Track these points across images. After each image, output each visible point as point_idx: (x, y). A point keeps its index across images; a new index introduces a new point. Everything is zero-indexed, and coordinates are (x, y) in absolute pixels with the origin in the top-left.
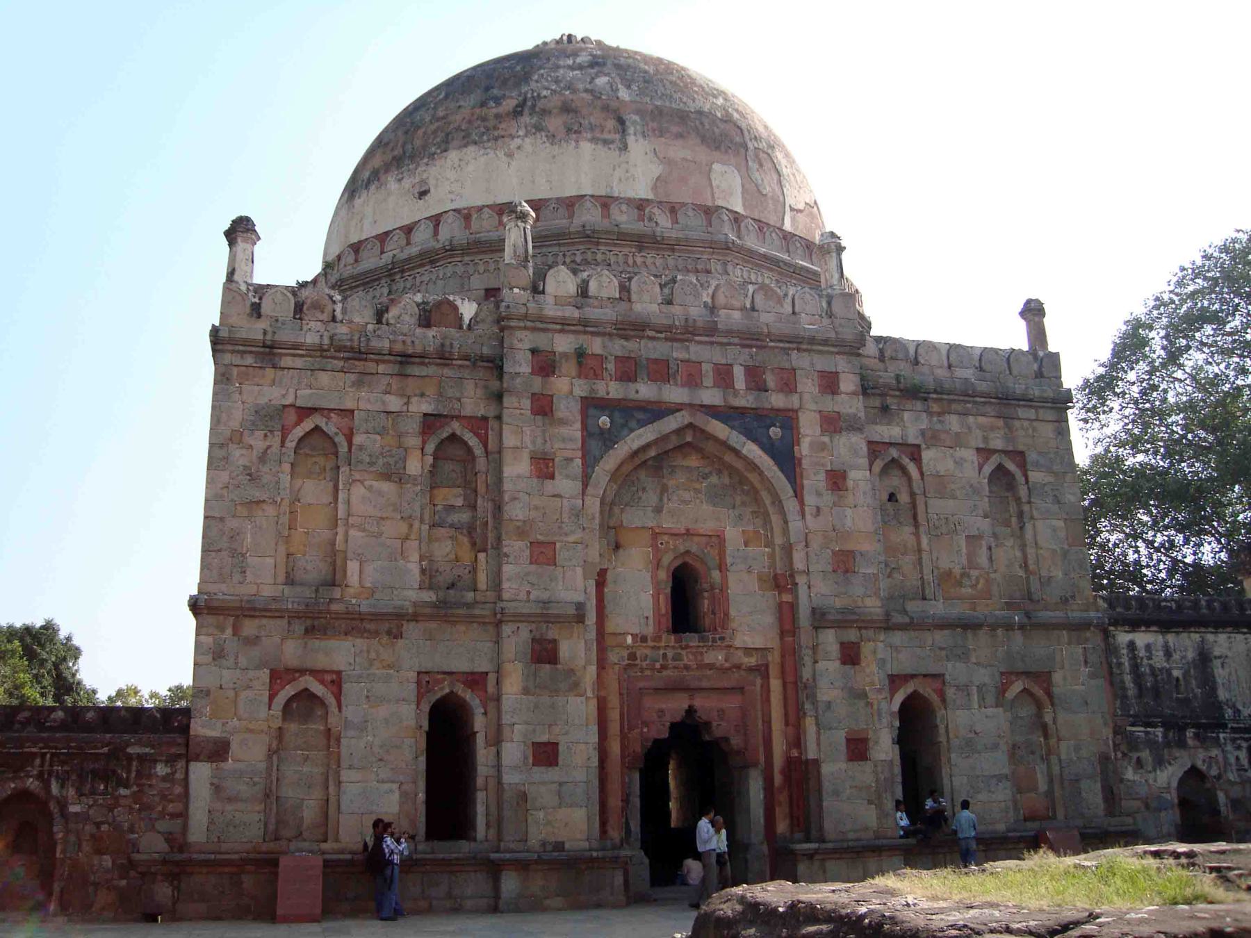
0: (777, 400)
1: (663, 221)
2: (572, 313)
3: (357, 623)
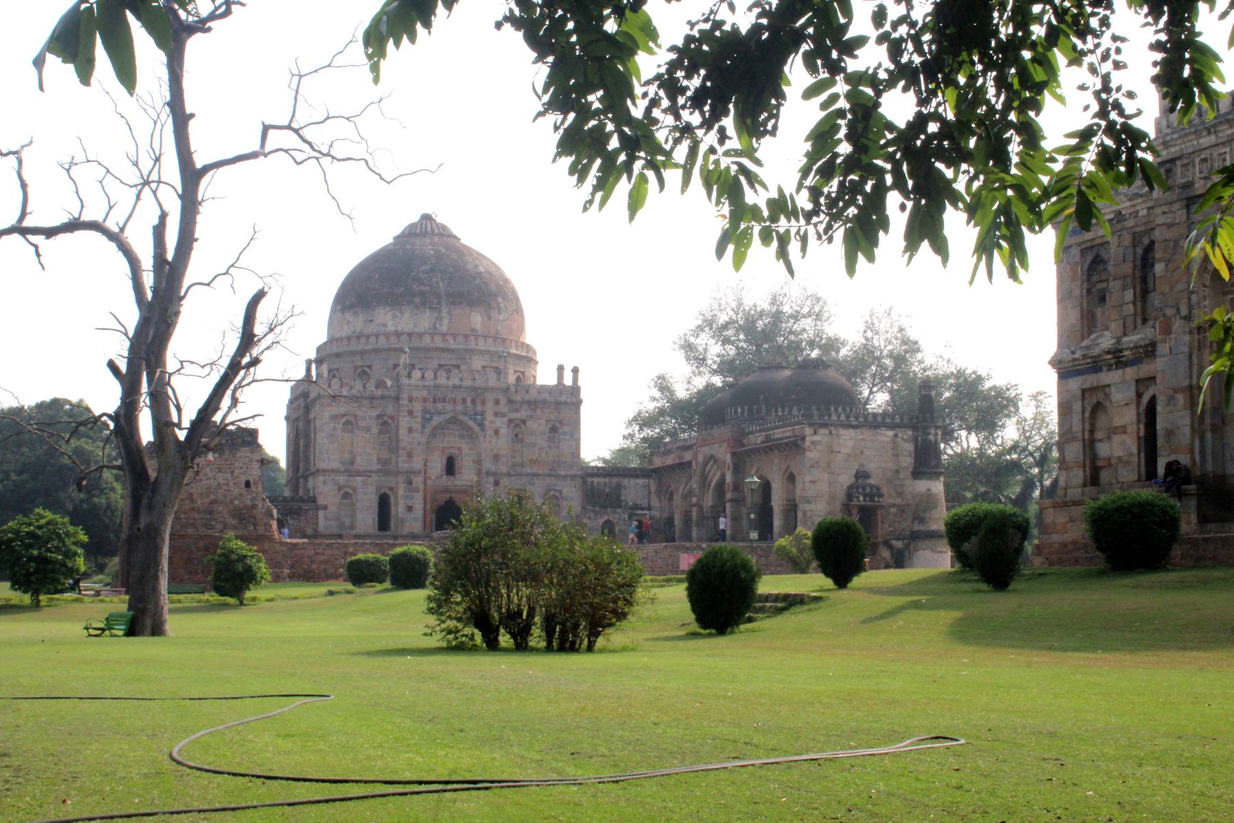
0: (479, 408)
1: (451, 340)
2: (420, 383)
3: (359, 474)
